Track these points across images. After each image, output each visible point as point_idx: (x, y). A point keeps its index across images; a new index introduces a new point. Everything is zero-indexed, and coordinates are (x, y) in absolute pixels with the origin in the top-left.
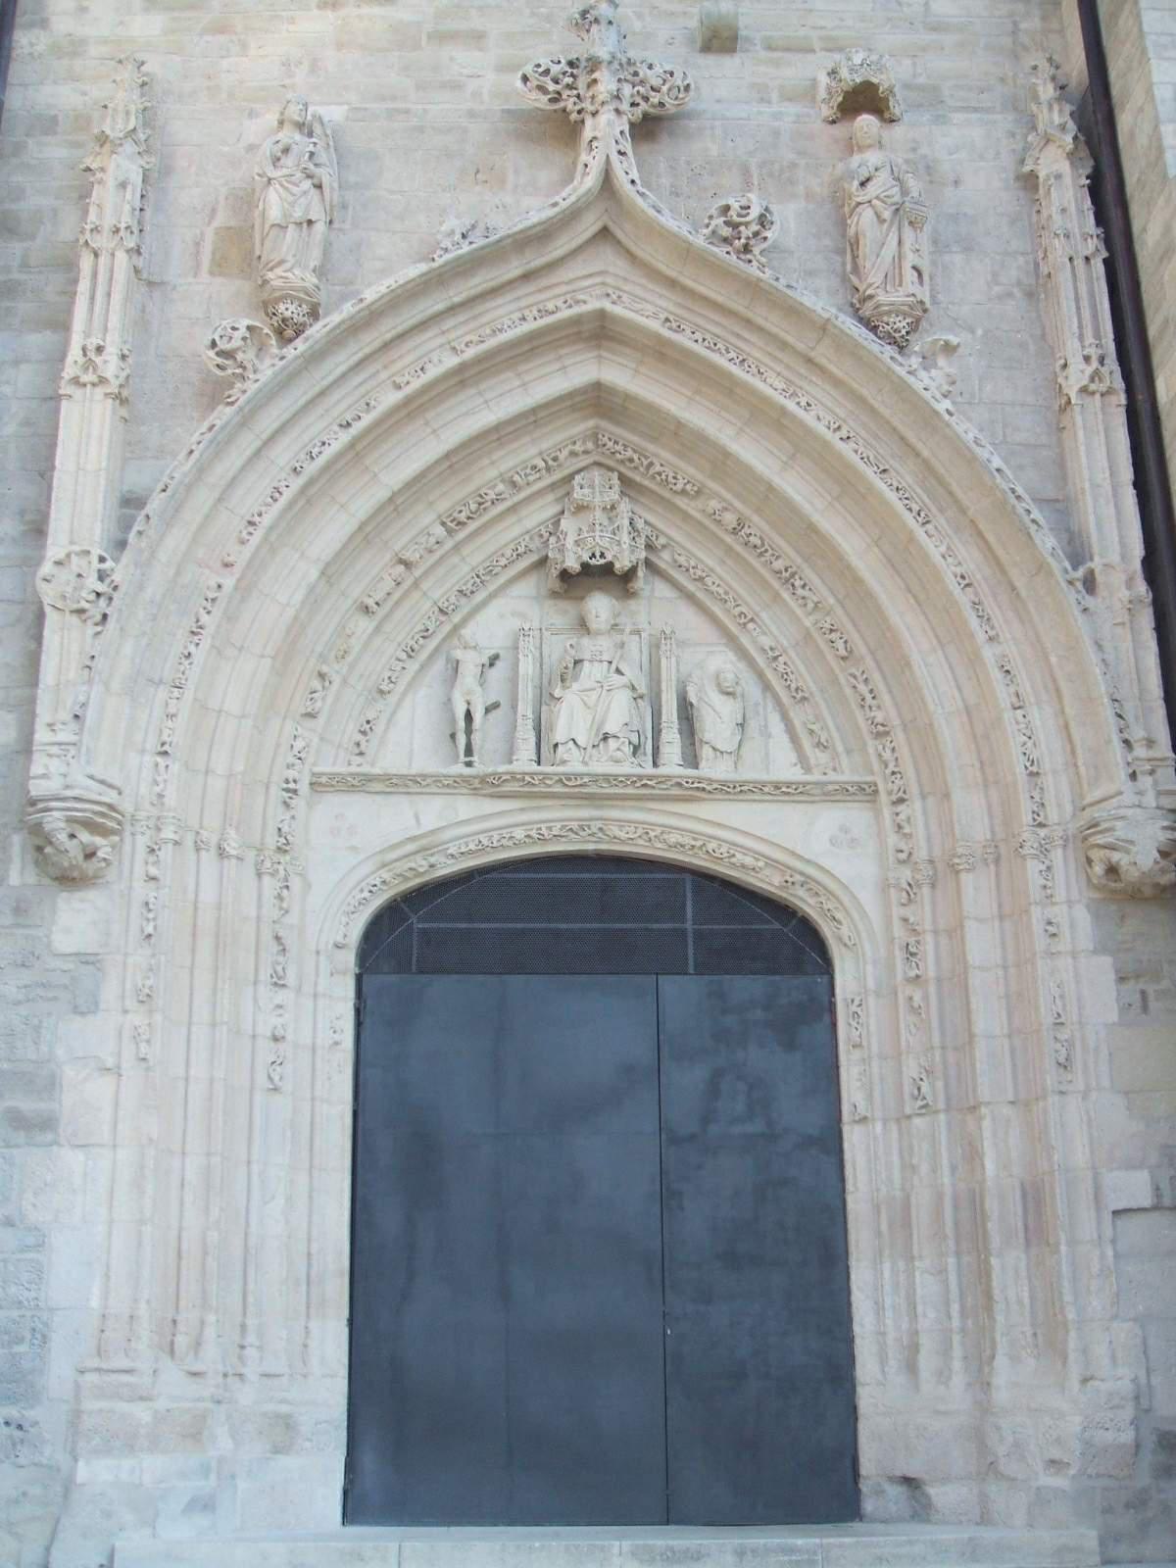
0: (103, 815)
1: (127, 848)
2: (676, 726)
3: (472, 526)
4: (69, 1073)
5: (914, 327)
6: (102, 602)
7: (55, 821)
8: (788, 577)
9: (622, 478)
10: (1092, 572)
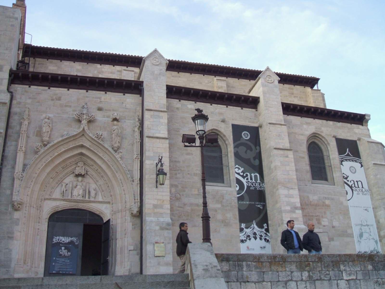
2: (88, 194)
3: (66, 168)
4: (15, 232)
5: (118, 149)
6: (22, 178)
7: (16, 204)
8: (102, 177)
9: (84, 163)
10: (133, 180)
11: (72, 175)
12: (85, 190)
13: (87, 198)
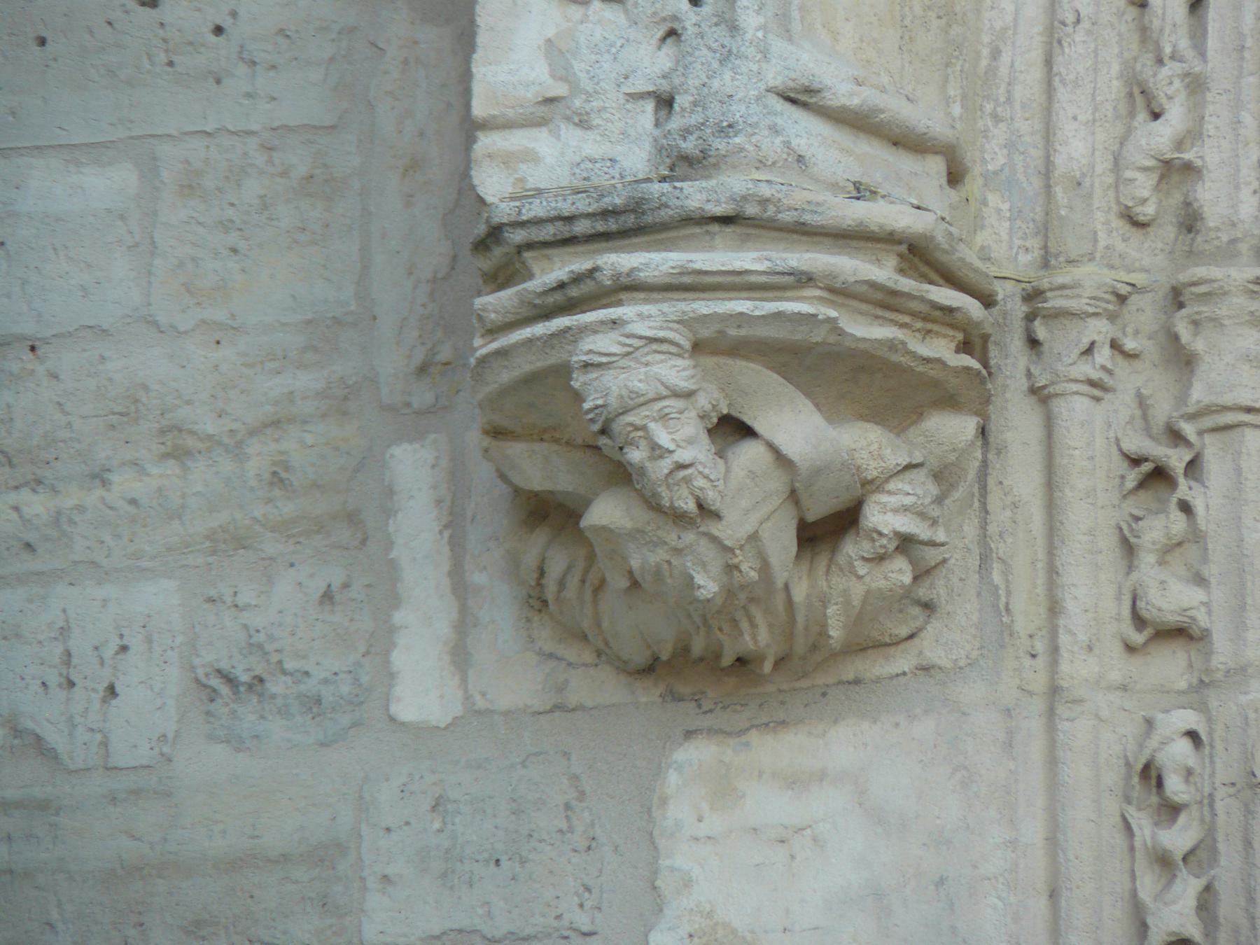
0: (885, 302)
1: (1020, 475)
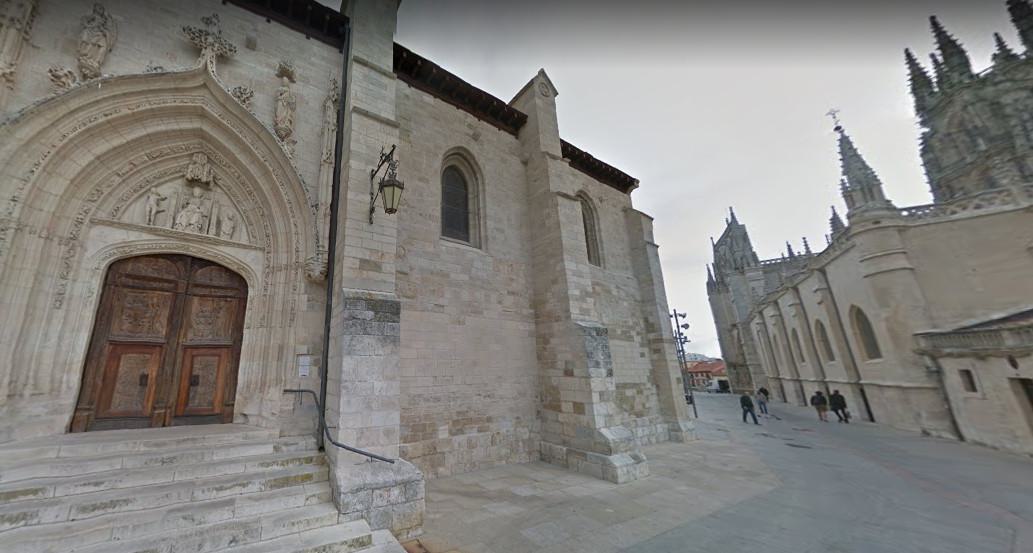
3: (158, 160)
11: (180, 181)
12: (207, 217)
13: (211, 236)
